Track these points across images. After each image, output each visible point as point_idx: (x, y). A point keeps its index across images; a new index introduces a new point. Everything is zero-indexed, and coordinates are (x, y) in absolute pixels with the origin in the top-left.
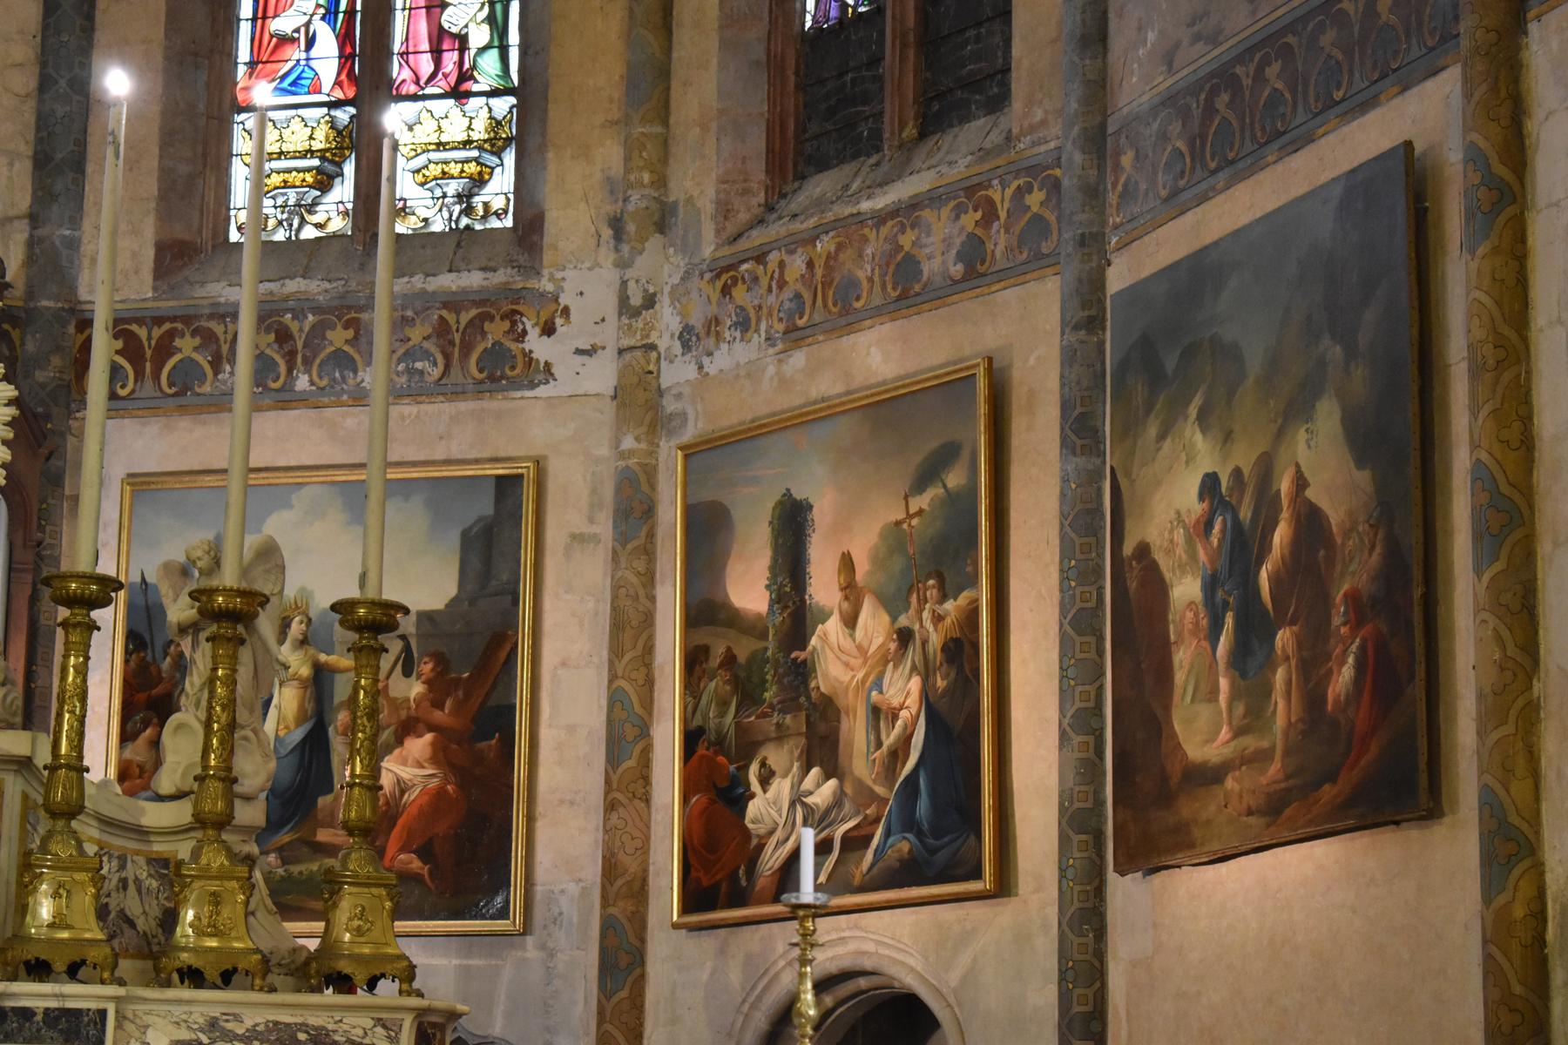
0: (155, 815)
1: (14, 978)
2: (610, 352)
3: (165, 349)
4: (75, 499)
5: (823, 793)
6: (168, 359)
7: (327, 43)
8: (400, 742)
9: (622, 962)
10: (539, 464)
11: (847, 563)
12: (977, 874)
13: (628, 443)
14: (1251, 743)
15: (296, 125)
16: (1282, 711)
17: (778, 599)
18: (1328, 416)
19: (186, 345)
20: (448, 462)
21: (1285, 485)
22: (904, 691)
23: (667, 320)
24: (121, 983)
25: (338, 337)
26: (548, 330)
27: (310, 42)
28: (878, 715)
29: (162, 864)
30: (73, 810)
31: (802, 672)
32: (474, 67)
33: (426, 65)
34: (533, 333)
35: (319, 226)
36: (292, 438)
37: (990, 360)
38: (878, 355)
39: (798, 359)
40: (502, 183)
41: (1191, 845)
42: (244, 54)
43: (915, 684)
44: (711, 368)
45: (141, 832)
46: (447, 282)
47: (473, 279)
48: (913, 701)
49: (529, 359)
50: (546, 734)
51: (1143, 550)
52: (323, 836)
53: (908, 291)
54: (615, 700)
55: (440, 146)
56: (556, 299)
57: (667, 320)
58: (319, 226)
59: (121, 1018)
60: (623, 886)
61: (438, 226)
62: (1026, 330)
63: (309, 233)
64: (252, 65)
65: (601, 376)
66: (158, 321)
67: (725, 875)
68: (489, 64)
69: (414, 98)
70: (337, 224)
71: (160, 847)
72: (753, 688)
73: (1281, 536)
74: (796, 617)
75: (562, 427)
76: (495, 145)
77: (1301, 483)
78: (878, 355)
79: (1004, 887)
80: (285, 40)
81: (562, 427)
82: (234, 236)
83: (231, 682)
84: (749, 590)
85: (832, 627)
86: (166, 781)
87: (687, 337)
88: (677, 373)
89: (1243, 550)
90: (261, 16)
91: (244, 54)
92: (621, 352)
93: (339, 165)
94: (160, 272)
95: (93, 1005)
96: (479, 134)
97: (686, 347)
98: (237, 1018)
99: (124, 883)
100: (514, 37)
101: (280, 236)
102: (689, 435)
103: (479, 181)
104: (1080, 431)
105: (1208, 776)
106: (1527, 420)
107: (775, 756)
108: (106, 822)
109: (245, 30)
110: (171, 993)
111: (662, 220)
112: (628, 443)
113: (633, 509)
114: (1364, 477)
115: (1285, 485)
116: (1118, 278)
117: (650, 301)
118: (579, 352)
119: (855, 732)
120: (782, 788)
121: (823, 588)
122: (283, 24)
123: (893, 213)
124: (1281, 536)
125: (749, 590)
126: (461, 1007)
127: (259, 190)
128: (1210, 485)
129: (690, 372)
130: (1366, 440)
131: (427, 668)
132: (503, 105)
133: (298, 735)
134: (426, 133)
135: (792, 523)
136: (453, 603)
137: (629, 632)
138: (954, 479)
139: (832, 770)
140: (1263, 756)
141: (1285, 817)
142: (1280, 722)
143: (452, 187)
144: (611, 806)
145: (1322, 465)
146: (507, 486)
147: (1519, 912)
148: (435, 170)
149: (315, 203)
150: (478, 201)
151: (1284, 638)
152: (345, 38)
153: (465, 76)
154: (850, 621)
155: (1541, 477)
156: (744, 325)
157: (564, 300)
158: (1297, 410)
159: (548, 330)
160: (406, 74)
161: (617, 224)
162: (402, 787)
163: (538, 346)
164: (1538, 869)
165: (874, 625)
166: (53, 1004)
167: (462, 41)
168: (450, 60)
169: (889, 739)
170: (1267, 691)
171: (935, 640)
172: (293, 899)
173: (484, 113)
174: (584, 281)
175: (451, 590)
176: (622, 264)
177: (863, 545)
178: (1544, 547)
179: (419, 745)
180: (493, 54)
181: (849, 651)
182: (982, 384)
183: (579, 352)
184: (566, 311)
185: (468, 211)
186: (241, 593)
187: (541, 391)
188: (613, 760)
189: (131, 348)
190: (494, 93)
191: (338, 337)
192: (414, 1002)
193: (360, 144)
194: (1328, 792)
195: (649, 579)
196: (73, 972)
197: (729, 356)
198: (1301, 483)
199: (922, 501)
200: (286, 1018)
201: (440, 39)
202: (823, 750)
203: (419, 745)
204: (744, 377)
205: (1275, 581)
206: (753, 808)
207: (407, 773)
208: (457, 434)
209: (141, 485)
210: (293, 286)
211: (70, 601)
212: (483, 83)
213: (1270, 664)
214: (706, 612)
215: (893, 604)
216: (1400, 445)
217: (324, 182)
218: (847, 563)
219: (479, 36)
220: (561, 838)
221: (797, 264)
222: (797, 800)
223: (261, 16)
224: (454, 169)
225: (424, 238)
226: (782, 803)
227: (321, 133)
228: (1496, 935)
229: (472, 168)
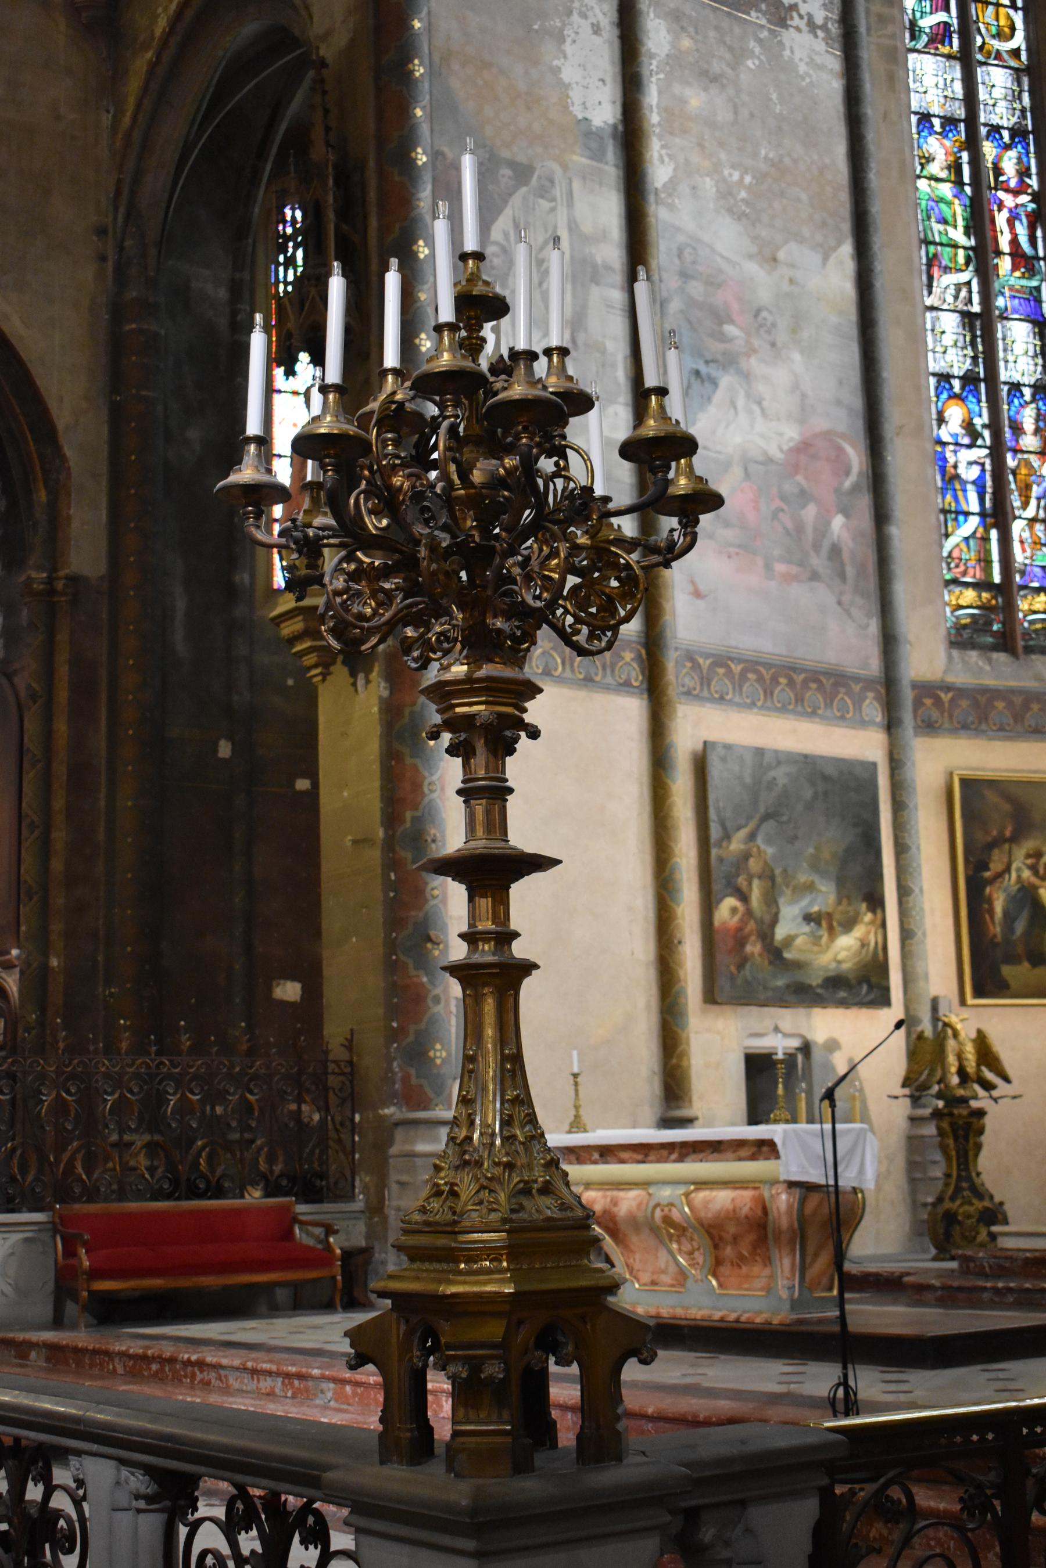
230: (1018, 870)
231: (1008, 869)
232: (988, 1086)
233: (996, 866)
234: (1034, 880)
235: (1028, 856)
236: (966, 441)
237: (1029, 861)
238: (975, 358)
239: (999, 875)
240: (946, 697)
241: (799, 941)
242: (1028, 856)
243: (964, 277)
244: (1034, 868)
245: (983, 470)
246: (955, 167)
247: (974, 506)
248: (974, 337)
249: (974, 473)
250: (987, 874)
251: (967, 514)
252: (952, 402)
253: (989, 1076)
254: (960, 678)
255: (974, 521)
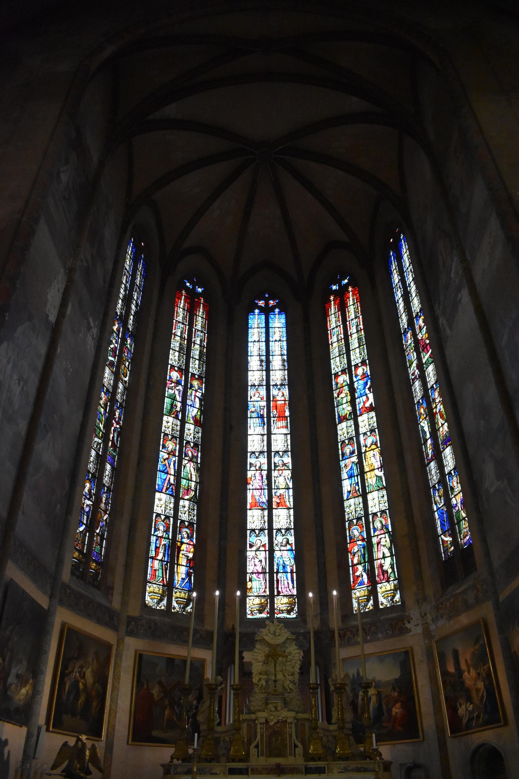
0: (332, 727)
1: (309, 761)
2: (421, 625)
3: (345, 635)
4: (335, 664)
5: (471, 708)
6: (348, 635)
7: (365, 576)
8: (395, 705)
9: (442, 745)
10: (412, 648)
11: (466, 660)
12: (500, 722)
13: (426, 642)
15: (362, 591)
17: (456, 669)
19: (348, 634)
20: (396, 649)
22: (480, 685)
23: (429, 617)
24: (328, 761)
25: (373, 628)
26: (409, 622)
27: (362, 576)
28: (478, 690)
29: (334, 737)
30: (316, 728)
31: (463, 683)
32: (390, 576)
33: (382, 577)
34: (407, 623)
35: (368, 609)
36: (370, 648)
37: (483, 618)
38: (464, 620)
39: (452, 622)
40: (397, 597)
42: (352, 580)
43: (482, 683)
44: (438, 626)
45: (330, 731)
46: (391, 616)
47: (394, 615)
48: (482, 687)
49: (406, 628)
50: (421, 700)
51: (515, 652)
52: (384, 725)
53: (467, 607)
54: (433, 693)
55: (386, 591)
56: (409, 616)
57: (429, 617)
58: (368, 609)
59: (328, 768)
60: (440, 729)
61: (388, 606)
62: (487, 611)
63: (367, 610)
64: (353, 582)
65: (419, 630)
66: (343, 630)
67: (457, 726)
68: (392, 575)
69: (381, 583)
70: (371, 608)
71: (334, 734)
72: (455, 687)
74: (459, 672)
75: (414, 639)
76: (395, 590)
78: (464, 620)
79: (506, 724)
80: (358, 577)
81: (414, 639)
82: (355, 612)
83: (341, 701)
84: (451, 669)
85: (466, 673)
86: (334, 720)
87: (433, 620)
88: (432, 627)
90: (354, 573)
91: (352, 580)
92: (422, 624)
93: (370, 597)
94: (343, 621)
95: (323, 766)
96: (392, 588)
97: (433, 622)
98: (349, 767)
99: (328, 741)
100: (396, 570)
101: (362, 611)
102: (436, 639)
103: (394, 597)
104: (502, 630)
107: (462, 701)
108: (323, 729)
109: (351, 576)
110: (336, 762)
111: (425, 599)
112: (426, 642)
113: (429, 654)
116: (501, 598)
117: (425, 614)
118: (415, 625)
119: (474, 693)
120: (463, 707)
121: (463, 667)
122: (358, 574)
123: (461, 592)
125: (451, 669)
126: (393, 761)
127: (359, 604)
129: (435, 627)
131: (397, 689)
132: (396, 582)
133: (377, 705)
134: (383, 589)
135: (456, 654)
136: (400, 676)
137: (433, 678)
138: (481, 642)
139: (471, 703)
143: (389, 598)
144: (435, 714)
146: (406, 653)
148: (386, 595)
149: (367, 604)
150: (394, 600)
152: (368, 575)
153: (389, 578)
154: (469, 672)
156: (442, 617)
157: (411, 616)
159: (409, 622)
160: (379, 579)
161: (417, 601)
162: (396, 713)
163: (408, 625)
165: (473, 673)
166: (316, 766)
167: (387, 572)
168: (386, 575)
169: (480, 695)
171: (484, 675)
172: (360, 741)
173: (393, 584)
174: (414, 613)
175: (399, 674)
176: (420, 608)
177: (468, 657)
179: (398, 705)
180: (393, 573)
181: (469, 677)
182: (482, 623)
183: (415, 625)
184: (412, 618)
185: (393, 602)
186: (341, 684)
187: (409, 634)
188: (434, 704)
189: (340, 636)
190: (393, 580)
191: (373, 628)
192: (382, 761)
193: (373, 592)
195: (434, 668)
196: (319, 759)
197: (441, 623)
199: (477, 647)
200: (359, 766)
201: (384, 572)
202: (469, 699)
203: (398, 705)
204: (444, 626)
206: (460, 711)
207: (397, 711)
208: (396, 644)
209: (344, 660)
210: (365, 620)
211: (312, 689)
212: (392, 579)
214: (445, 673)
215: (475, 668)
217: (368, 600)
218: (466, 660)
219: (390, 571)
220: (427, 721)
221: (448, 604)
222: (466, 709)
223: (354, 573)
224: (389, 595)
225: (386, 608)
226: (464, 709)
227: (366, 592)
229: (392, 594)
230: (76, 672)
231: (72, 672)
232: (89, 773)
233: (70, 669)
234: (79, 677)
235: (79, 667)
236: (88, 497)
237: (79, 669)
238: (96, 469)
239: (70, 673)
240: (69, 591)
241: (13, 686)
242: (79, 667)
243: (100, 441)
244: (80, 672)
245: (90, 509)
246: (106, 405)
247: (85, 522)
248: (98, 462)
249: (87, 509)
250: (67, 671)
251: (84, 524)
252: (88, 481)
253: (91, 767)
254: (73, 586)
255: (84, 527)
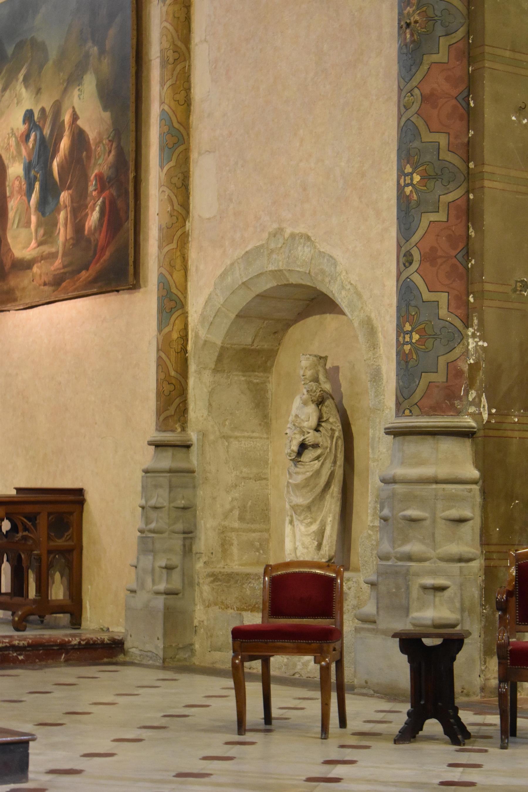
14: (46, 249)
16: (63, 233)
18: (90, 83)
21: (67, 118)
41: (15, 300)
73: (64, 144)
77: (75, 117)
89: (45, 150)
105: (25, 265)
106: (188, 90)
114: (107, 115)
115: (67, 118)
124: (64, 144)
128: (29, 116)
130: (108, 97)
140: (53, 256)
141: (63, 286)
142: (61, 239)
145: (86, 109)
147: (175, 336)
151: (65, 196)
155: (194, 119)
158: (74, 79)
164: (185, 315)
170: (55, 224)
178: (194, 155)
194: (84, 275)
198: (75, 117)
205: (61, 167)
213: (57, 210)
216: (126, 100)
228: (164, 347)
